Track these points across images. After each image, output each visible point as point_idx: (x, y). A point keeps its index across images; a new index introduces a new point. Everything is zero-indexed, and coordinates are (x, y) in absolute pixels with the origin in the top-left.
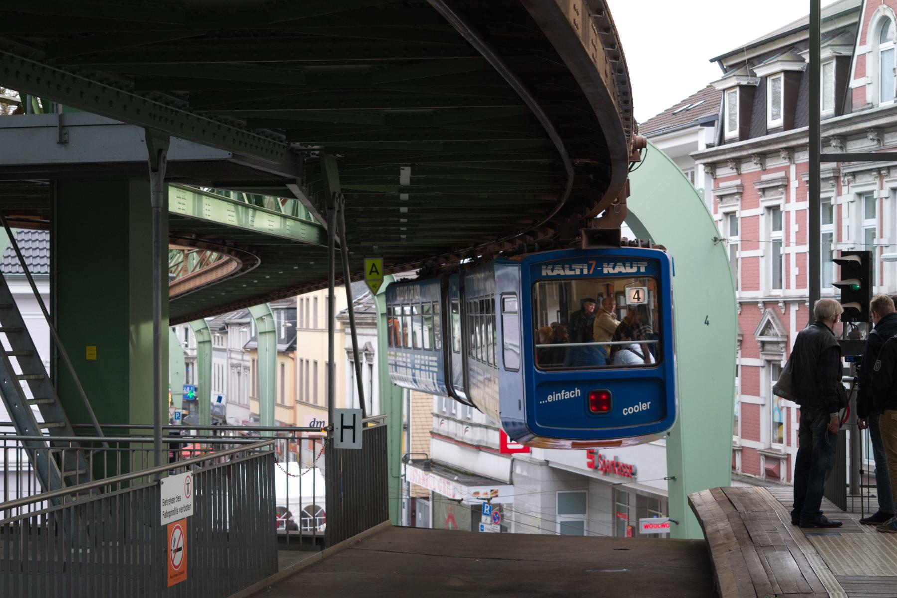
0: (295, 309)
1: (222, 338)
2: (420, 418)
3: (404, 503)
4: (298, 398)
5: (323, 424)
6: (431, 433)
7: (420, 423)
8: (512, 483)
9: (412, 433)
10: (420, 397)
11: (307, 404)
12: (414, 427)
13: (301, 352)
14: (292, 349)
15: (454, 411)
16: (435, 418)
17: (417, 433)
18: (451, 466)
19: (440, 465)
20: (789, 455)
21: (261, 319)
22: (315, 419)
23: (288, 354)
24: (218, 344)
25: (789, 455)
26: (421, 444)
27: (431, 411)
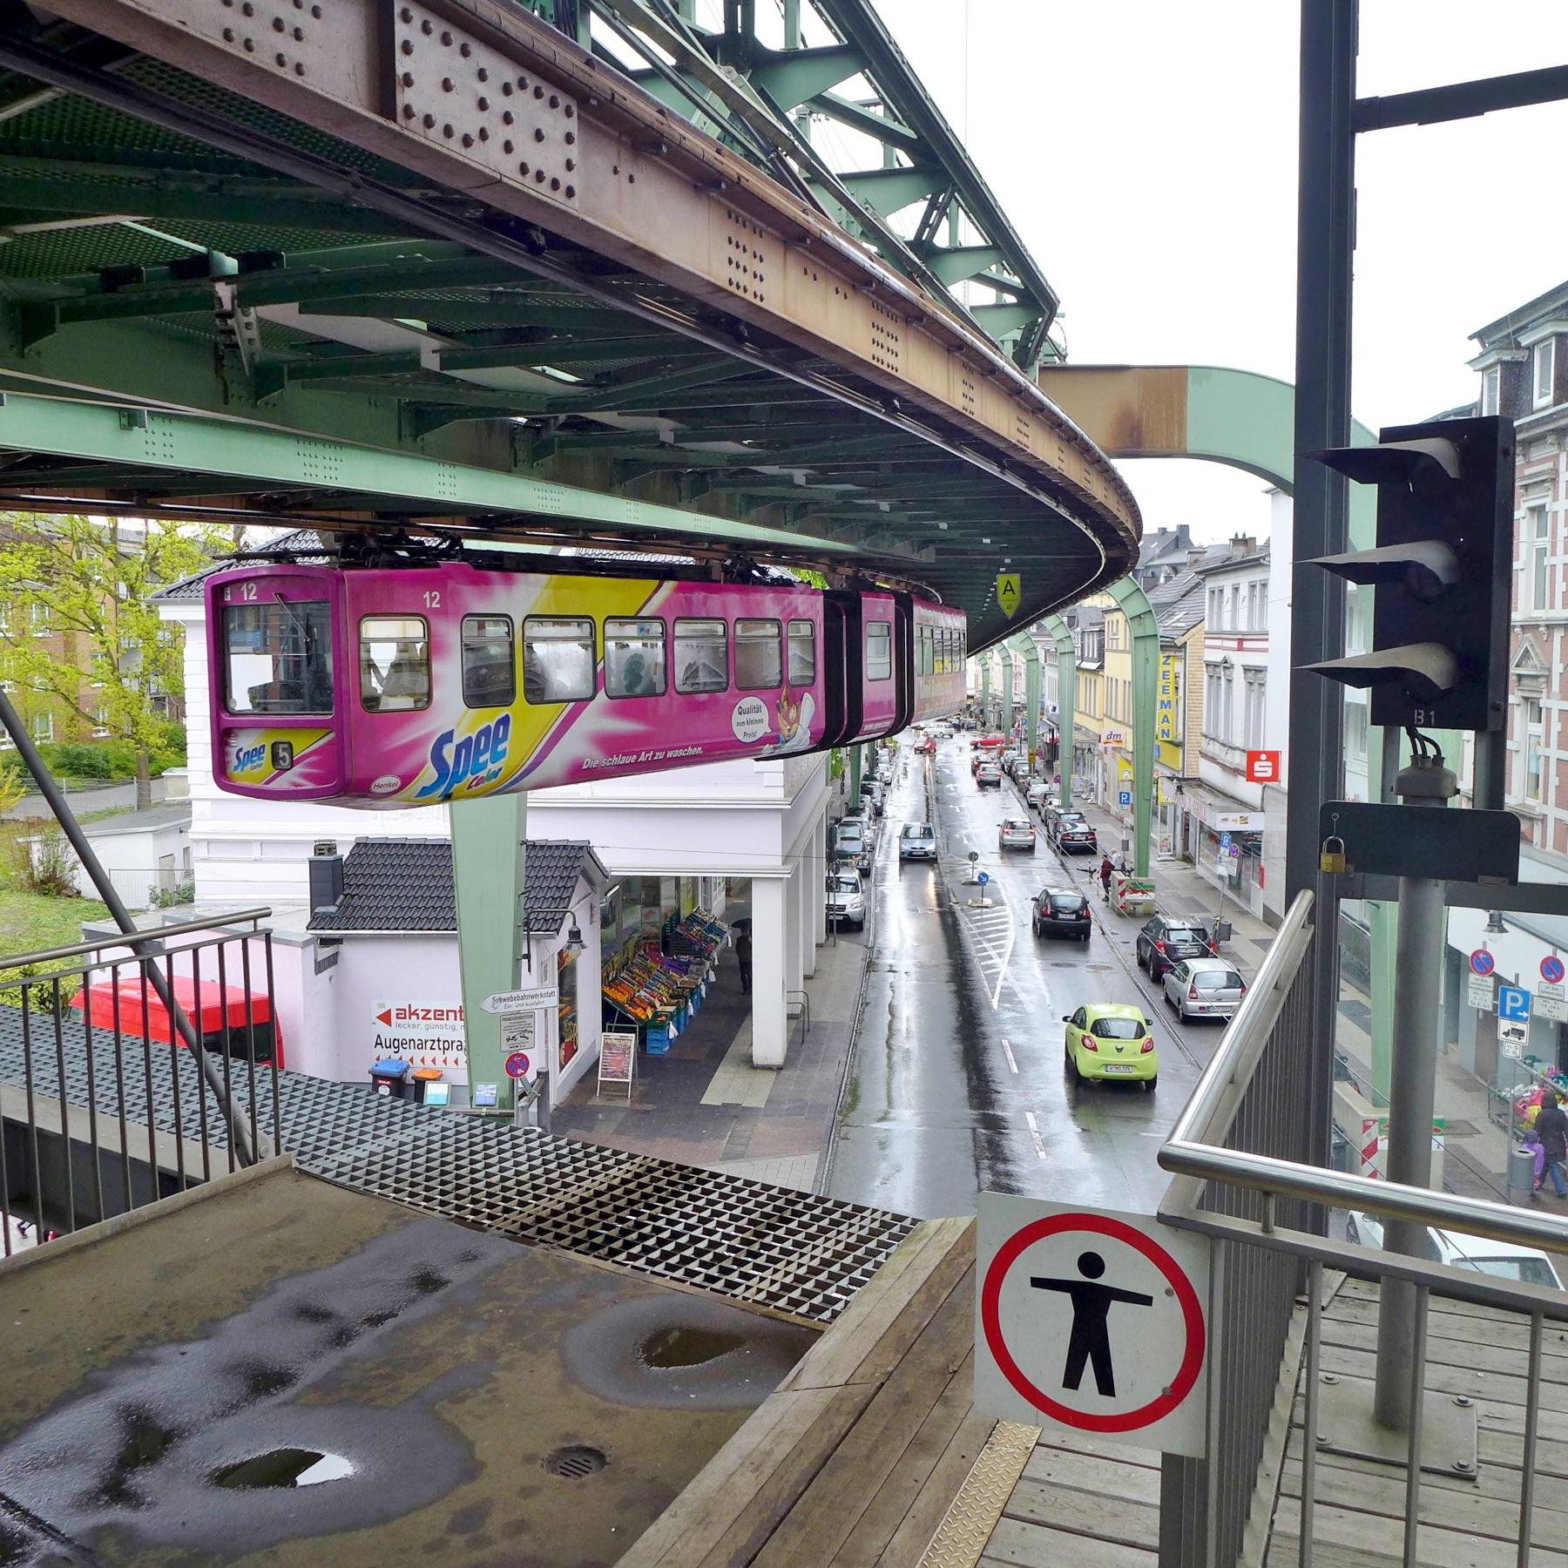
8: (1262, 811)
11: (1110, 718)
13: (1107, 671)
14: (1101, 667)
20: (1545, 816)
25: (1545, 816)
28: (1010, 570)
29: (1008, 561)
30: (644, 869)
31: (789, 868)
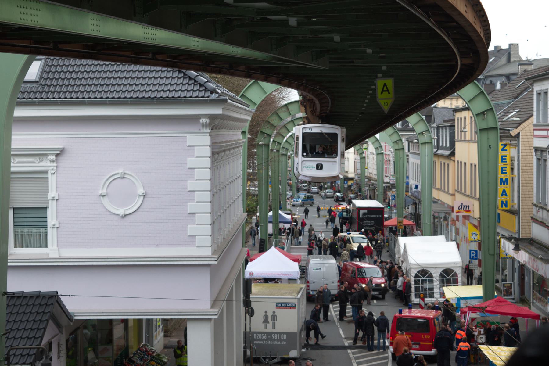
0: (455, 126)
1: (419, 146)
2: (527, 206)
3: (516, 269)
4: (456, 189)
5: (468, 207)
6: (532, 218)
7: (527, 210)
9: (521, 217)
10: (527, 190)
11: (460, 192)
12: (523, 213)
14: (453, 154)
15: (546, 203)
16: (534, 207)
17: (526, 217)
18: (544, 244)
19: (537, 243)
21: (422, 133)
22: (462, 204)
23: (451, 157)
24: (415, 150)
26: (528, 225)
27: (532, 202)
28: (386, 75)
29: (384, 68)
30: (101, 314)
31: (216, 310)
